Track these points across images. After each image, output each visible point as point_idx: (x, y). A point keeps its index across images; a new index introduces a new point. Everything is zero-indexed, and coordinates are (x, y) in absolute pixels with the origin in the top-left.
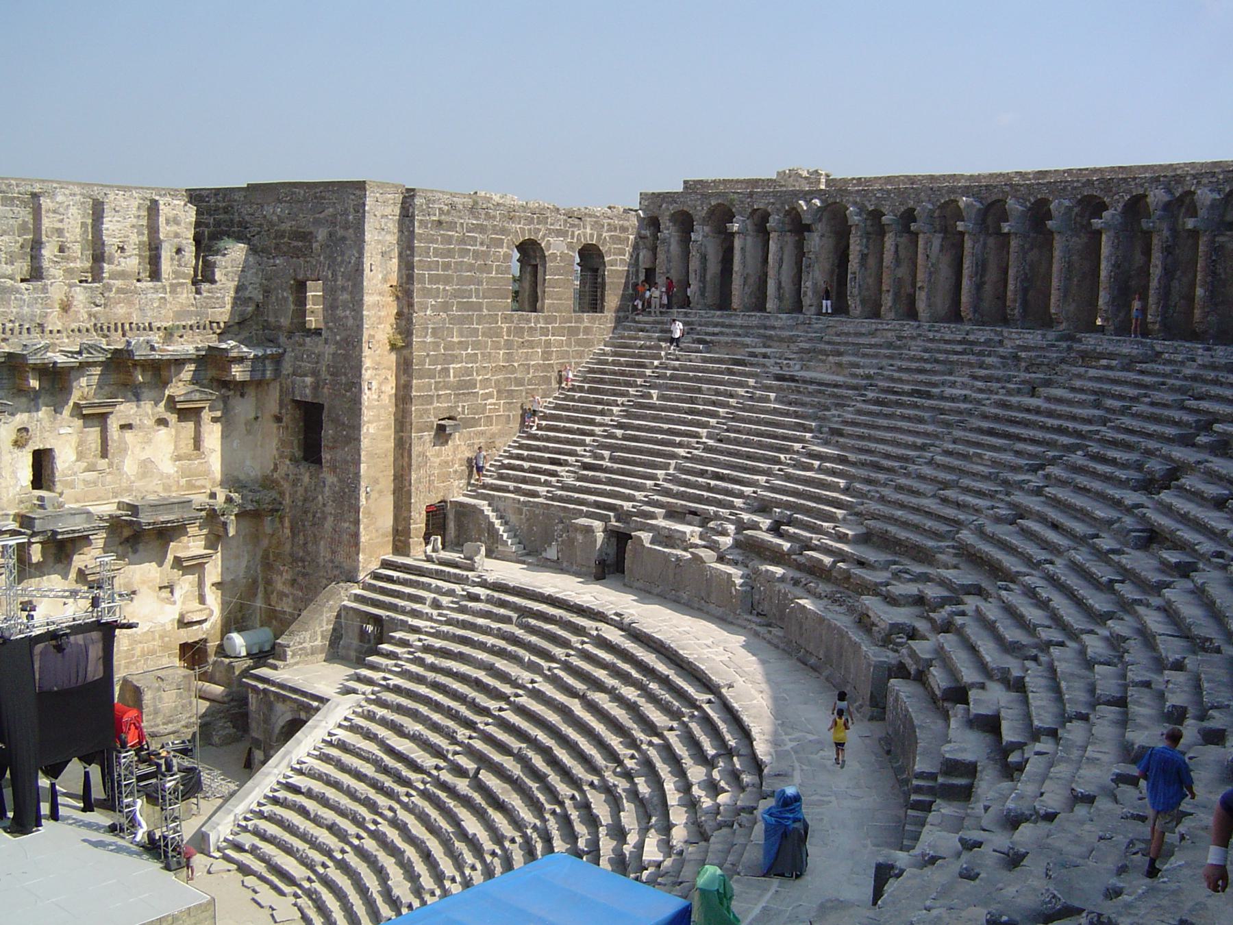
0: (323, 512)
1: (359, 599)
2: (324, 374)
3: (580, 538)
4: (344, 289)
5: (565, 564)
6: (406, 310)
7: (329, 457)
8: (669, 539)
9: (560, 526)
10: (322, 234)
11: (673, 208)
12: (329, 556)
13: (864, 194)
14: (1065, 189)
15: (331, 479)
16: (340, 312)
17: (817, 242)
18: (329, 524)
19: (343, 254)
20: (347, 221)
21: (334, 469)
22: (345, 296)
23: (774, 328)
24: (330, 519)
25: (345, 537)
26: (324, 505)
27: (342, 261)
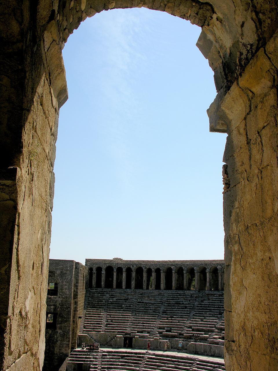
0: (56, 340)
1: (70, 360)
2: (58, 305)
3: (118, 339)
4: (65, 285)
5: (114, 346)
6: (76, 290)
7: (59, 326)
8: (143, 337)
9: (109, 338)
10: (58, 272)
11: (97, 266)
12: (58, 351)
13: (146, 265)
14: (196, 265)
15: (59, 331)
16: (64, 291)
17: (154, 274)
18: (59, 343)
19: (65, 277)
20: (67, 269)
21: (61, 328)
22: (66, 287)
23: (128, 292)
24: (59, 342)
25: (65, 346)
26: (57, 338)
27: (65, 279)
